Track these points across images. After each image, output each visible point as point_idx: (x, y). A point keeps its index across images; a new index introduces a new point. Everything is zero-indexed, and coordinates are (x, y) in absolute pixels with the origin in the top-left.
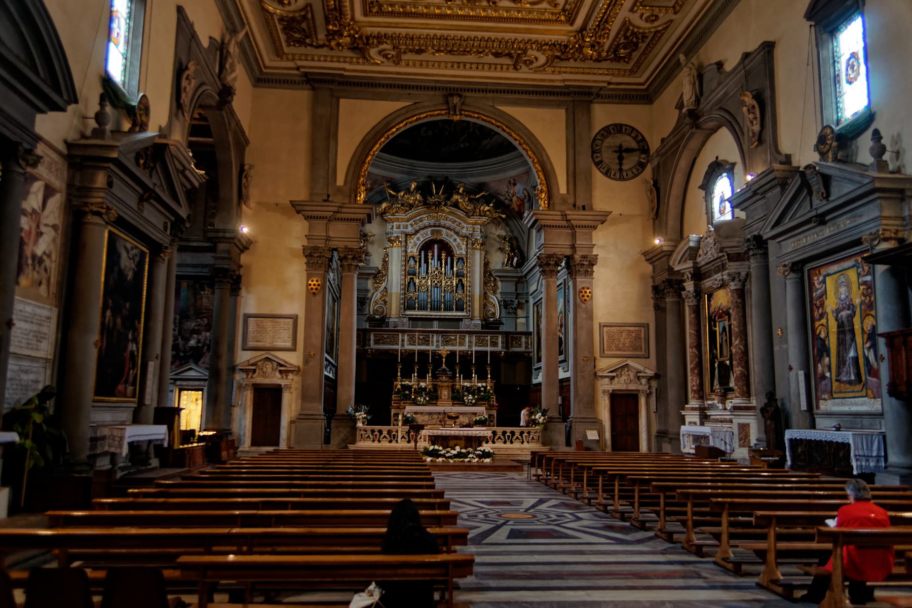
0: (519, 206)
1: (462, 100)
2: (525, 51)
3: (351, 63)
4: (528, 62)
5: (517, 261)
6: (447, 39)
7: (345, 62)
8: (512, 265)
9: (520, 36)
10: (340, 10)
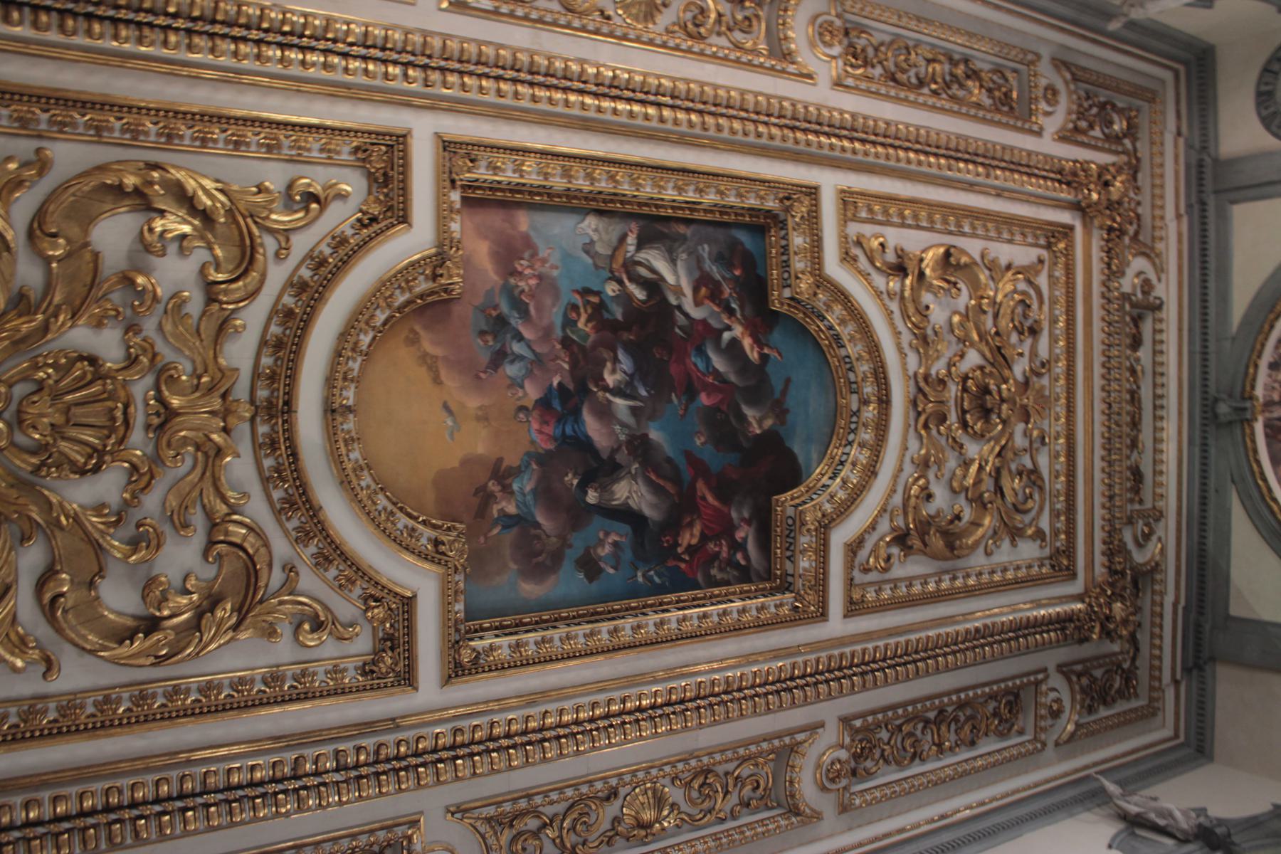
1: (1224, 396)
2: (1125, 297)
3: (1162, 594)
4: (1146, 288)
6: (1109, 439)
7: (1162, 605)
9: (1097, 313)
10: (1065, 621)
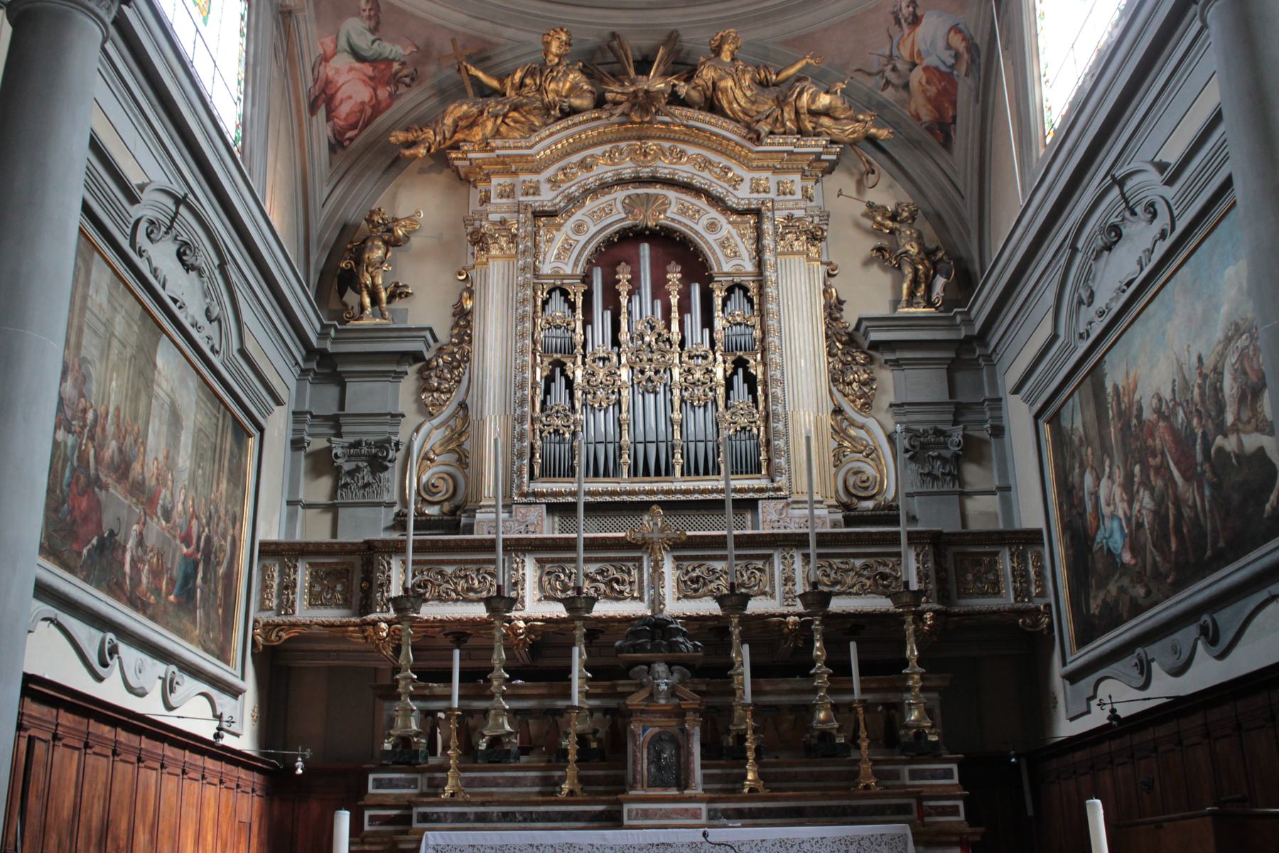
0: (935, 103)
5: (945, 289)
8: (930, 303)
